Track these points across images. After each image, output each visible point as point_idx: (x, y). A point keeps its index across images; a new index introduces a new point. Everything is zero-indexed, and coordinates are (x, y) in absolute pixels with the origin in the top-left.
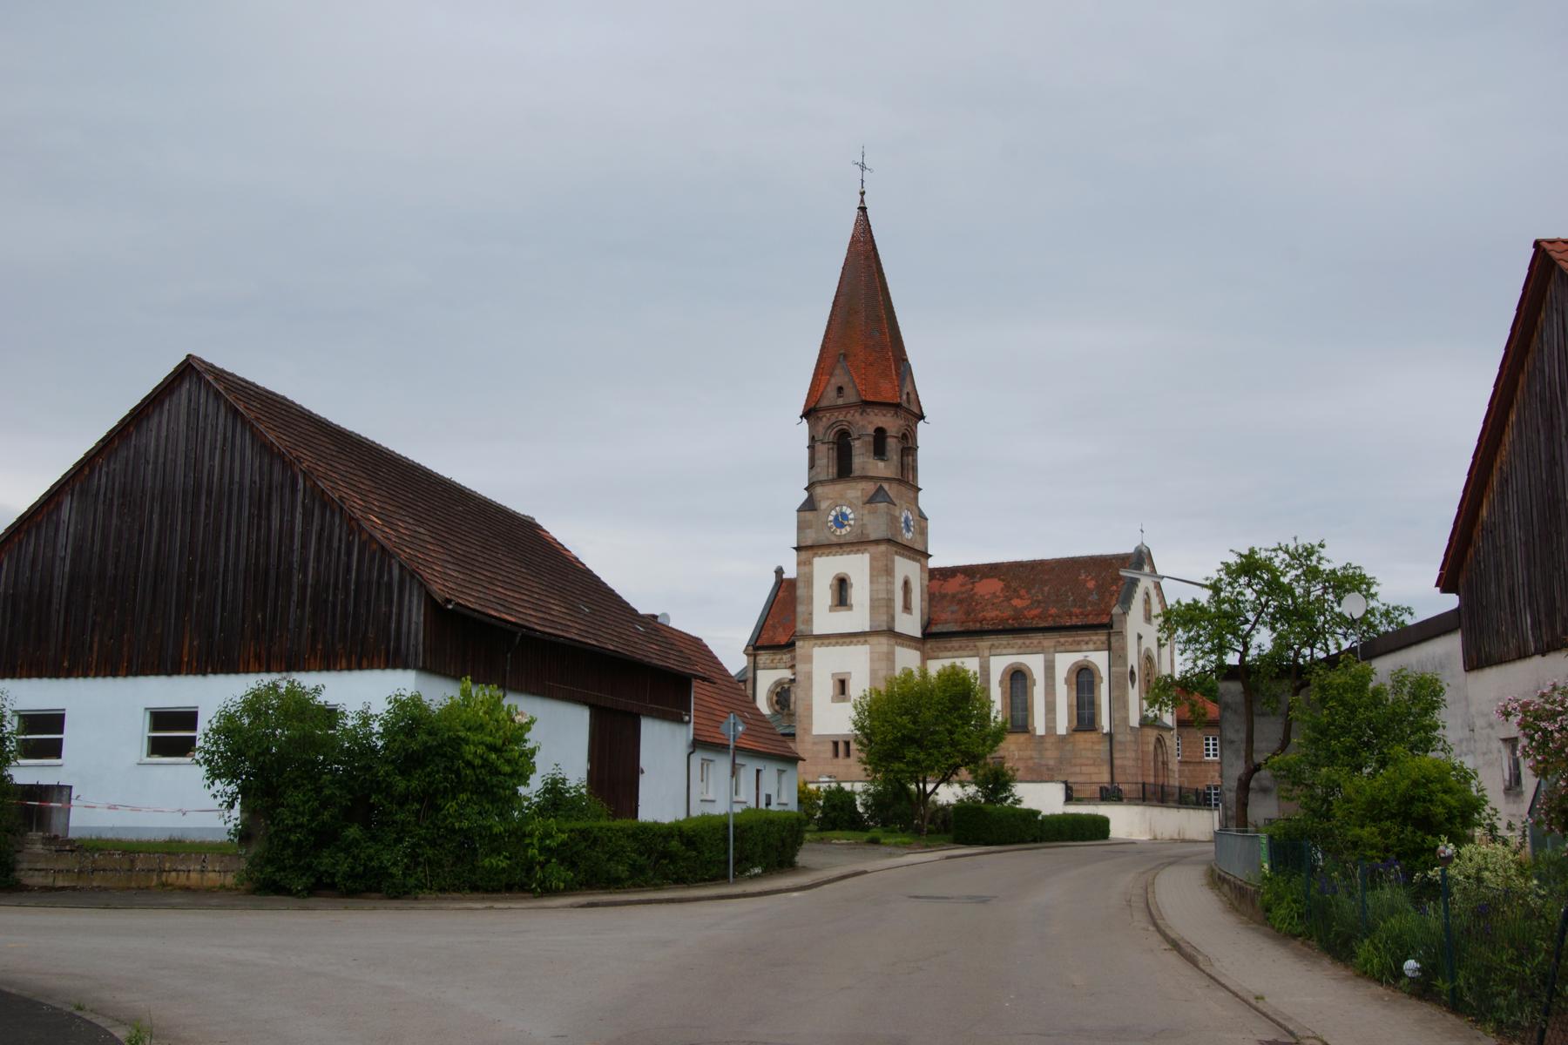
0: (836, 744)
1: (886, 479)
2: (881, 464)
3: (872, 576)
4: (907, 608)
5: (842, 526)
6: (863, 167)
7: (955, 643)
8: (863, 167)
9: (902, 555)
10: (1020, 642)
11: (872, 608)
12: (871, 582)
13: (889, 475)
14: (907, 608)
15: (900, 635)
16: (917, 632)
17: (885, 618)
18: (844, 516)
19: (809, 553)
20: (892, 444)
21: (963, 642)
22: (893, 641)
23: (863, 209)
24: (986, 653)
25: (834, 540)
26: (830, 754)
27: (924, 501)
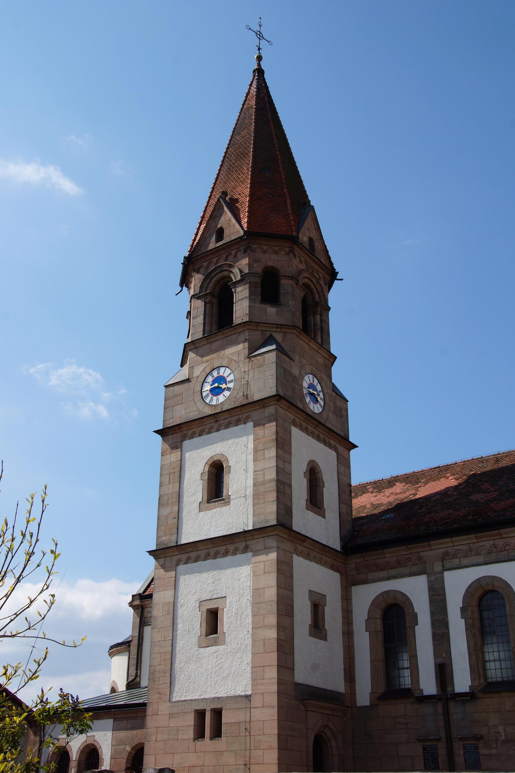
0: (200, 715)
1: (278, 326)
2: (271, 310)
3: (256, 451)
4: (315, 502)
5: (216, 391)
6: (260, 36)
7: (391, 555)
8: (260, 36)
9: (306, 430)
10: (488, 544)
11: (256, 496)
12: (255, 460)
13: (282, 321)
14: (315, 502)
15: (300, 539)
16: (334, 542)
17: (273, 508)
18: (221, 379)
19: (177, 436)
20: (291, 294)
21: (401, 552)
22: (288, 546)
23: (259, 72)
24: (438, 567)
25: (208, 411)
26: (190, 733)
27: (339, 375)
